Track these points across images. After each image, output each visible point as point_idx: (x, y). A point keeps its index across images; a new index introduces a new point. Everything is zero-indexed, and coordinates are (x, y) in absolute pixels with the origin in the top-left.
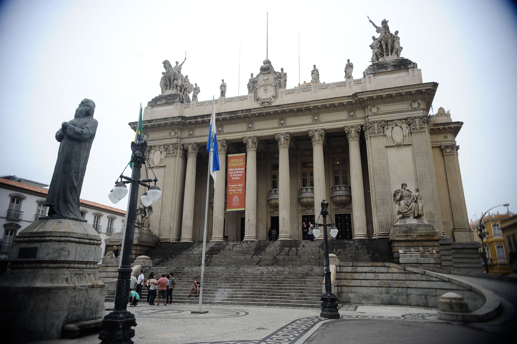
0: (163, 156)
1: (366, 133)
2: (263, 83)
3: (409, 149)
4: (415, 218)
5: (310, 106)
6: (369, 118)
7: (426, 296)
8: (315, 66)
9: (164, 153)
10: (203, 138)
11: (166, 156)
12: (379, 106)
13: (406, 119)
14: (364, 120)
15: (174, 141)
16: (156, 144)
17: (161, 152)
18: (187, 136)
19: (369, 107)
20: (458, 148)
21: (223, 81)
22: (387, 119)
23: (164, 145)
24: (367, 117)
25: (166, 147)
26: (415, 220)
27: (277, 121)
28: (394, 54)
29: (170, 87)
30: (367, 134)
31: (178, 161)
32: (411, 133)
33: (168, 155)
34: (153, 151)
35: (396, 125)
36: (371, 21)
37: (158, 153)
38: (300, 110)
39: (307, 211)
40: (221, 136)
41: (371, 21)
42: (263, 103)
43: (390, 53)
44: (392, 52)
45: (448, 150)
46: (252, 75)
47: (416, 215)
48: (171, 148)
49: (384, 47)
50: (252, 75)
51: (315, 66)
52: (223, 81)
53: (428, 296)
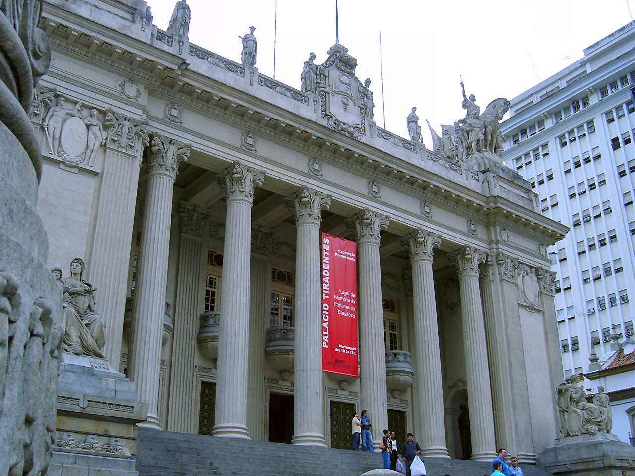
0: (95, 144)
1: (490, 270)
3: (539, 317)
5: (431, 182)
6: (500, 246)
8: (414, 109)
9: (98, 136)
10: (206, 143)
11: (104, 146)
12: (510, 233)
13: (537, 270)
14: (487, 246)
15: (137, 114)
16: (73, 96)
17: (88, 127)
18: (161, 116)
19: (498, 228)
21: (253, 29)
22: (521, 260)
23: (104, 113)
24: (497, 243)
25: (107, 120)
27: (364, 182)
30: (494, 272)
31: (126, 172)
33: (113, 146)
34: (59, 113)
35: (527, 274)
36: (462, 84)
38: (412, 182)
39: (340, 392)
40: (252, 160)
41: (462, 84)
46: (313, 56)
48: (125, 130)
49: (489, 137)
50: (313, 56)
51: (414, 109)
52: (253, 29)
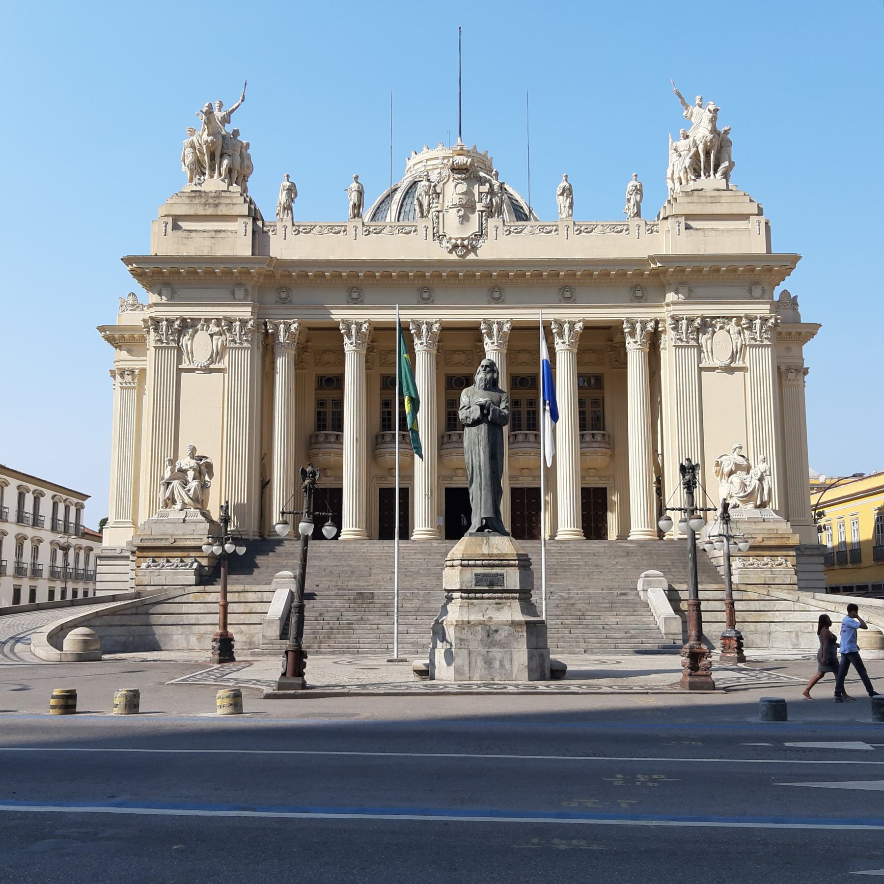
2: (456, 201)
4: (756, 507)
7: (797, 636)
17: (211, 336)
20: (806, 372)
26: (758, 510)
28: (719, 175)
29: (212, 169)
30: (668, 341)
32: (746, 346)
37: (202, 336)
42: (455, 246)
43: (712, 172)
44: (715, 171)
45: (791, 376)
47: (759, 503)
53: (800, 633)
